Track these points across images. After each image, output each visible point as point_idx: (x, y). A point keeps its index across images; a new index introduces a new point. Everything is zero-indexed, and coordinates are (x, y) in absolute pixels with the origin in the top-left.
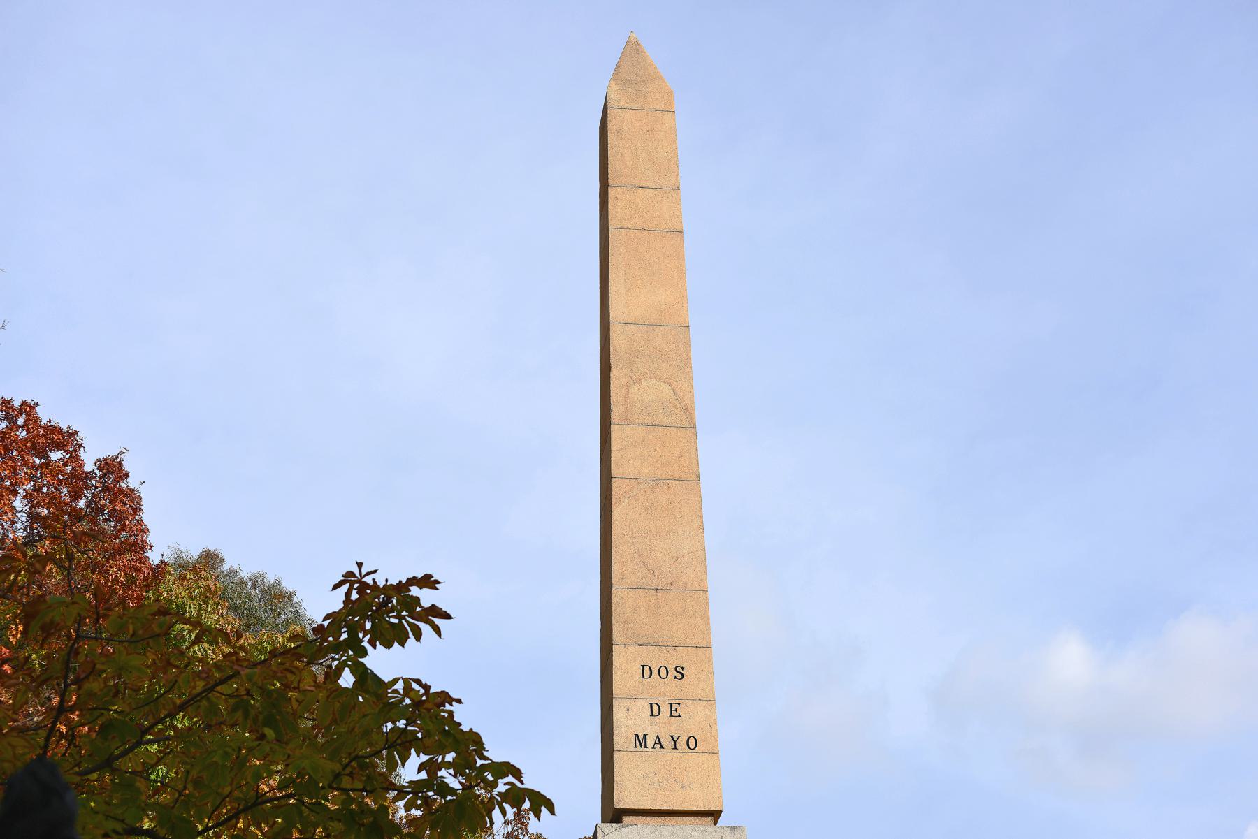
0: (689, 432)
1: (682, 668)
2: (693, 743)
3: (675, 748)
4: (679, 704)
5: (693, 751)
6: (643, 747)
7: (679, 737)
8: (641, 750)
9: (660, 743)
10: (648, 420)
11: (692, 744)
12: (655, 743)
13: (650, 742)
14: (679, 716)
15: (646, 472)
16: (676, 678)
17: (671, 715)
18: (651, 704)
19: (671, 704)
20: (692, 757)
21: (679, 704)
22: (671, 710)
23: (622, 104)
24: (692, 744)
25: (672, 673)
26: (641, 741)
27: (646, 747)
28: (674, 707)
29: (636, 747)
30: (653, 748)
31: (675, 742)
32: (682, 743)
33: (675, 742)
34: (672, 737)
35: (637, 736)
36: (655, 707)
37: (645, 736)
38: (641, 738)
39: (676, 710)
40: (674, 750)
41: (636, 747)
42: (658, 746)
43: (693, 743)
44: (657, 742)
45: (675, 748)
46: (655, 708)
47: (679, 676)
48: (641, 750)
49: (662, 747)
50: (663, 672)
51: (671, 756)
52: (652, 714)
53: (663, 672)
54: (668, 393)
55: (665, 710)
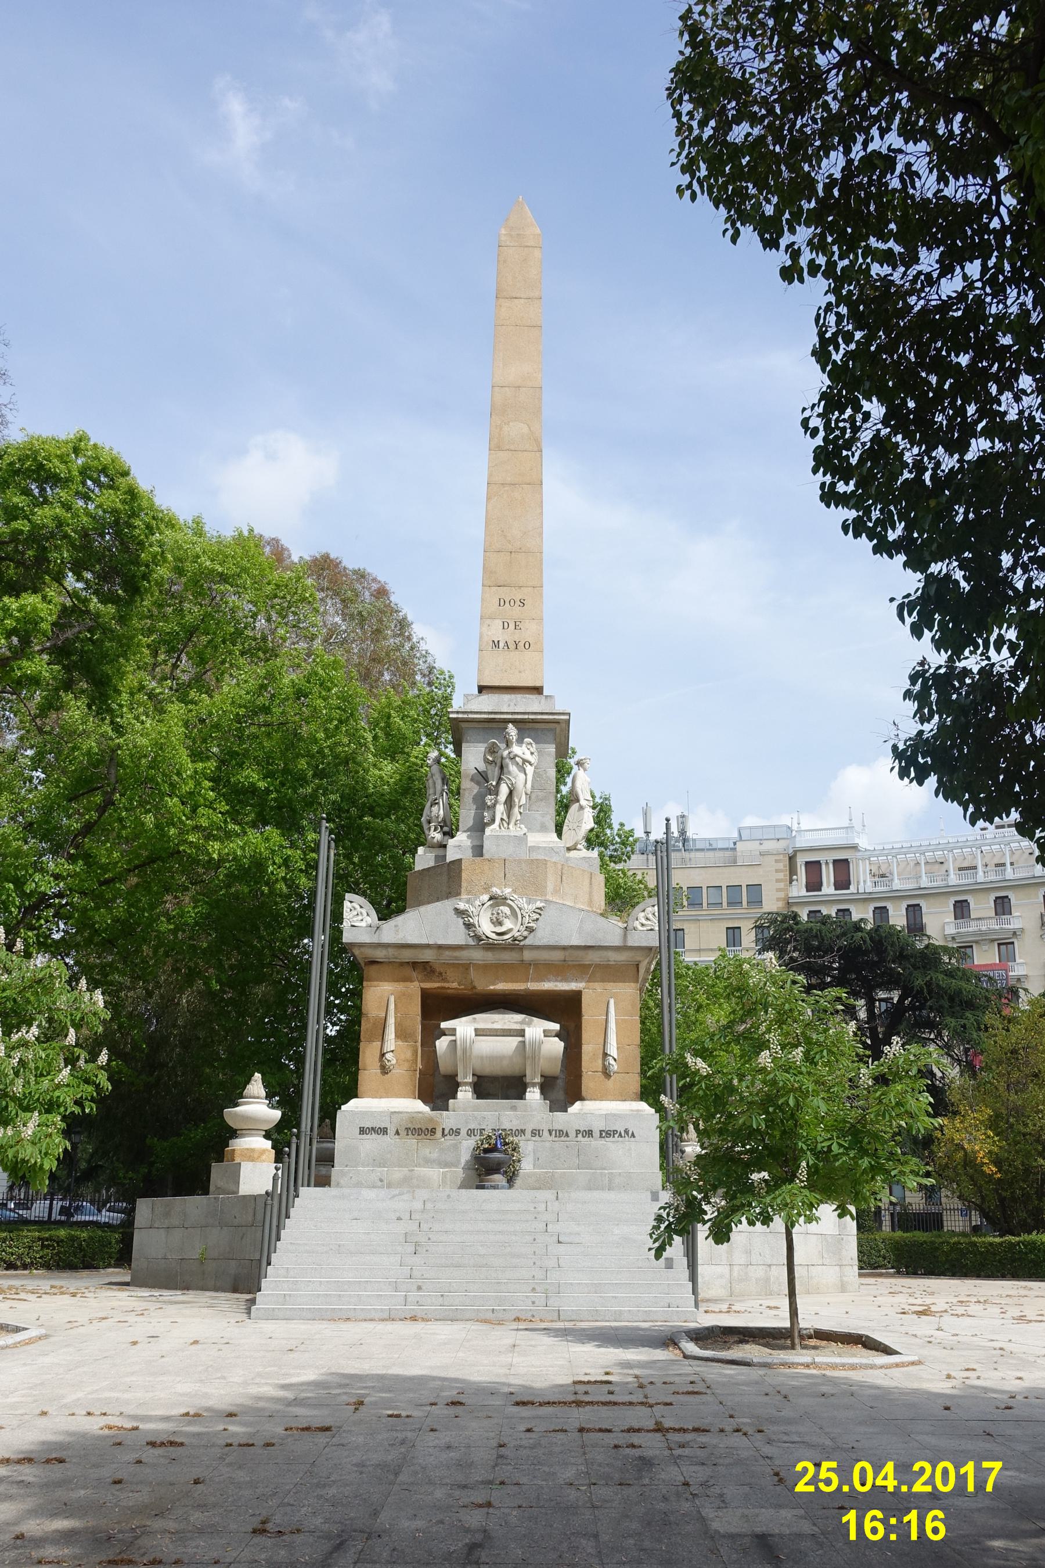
0: (538, 454)
2: (527, 646)
10: (512, 447)
11: (527, 646)
13: (501, 645)
15: (509, 480)
20: (526, 652)
23: (508, 243)
24: (527, 646)
32: (521, 644)
43: (527, 646)
50: (512, 602)
51: (514, 655)
53: (512, 602)
54: (525, 429)
55: (512, 626)
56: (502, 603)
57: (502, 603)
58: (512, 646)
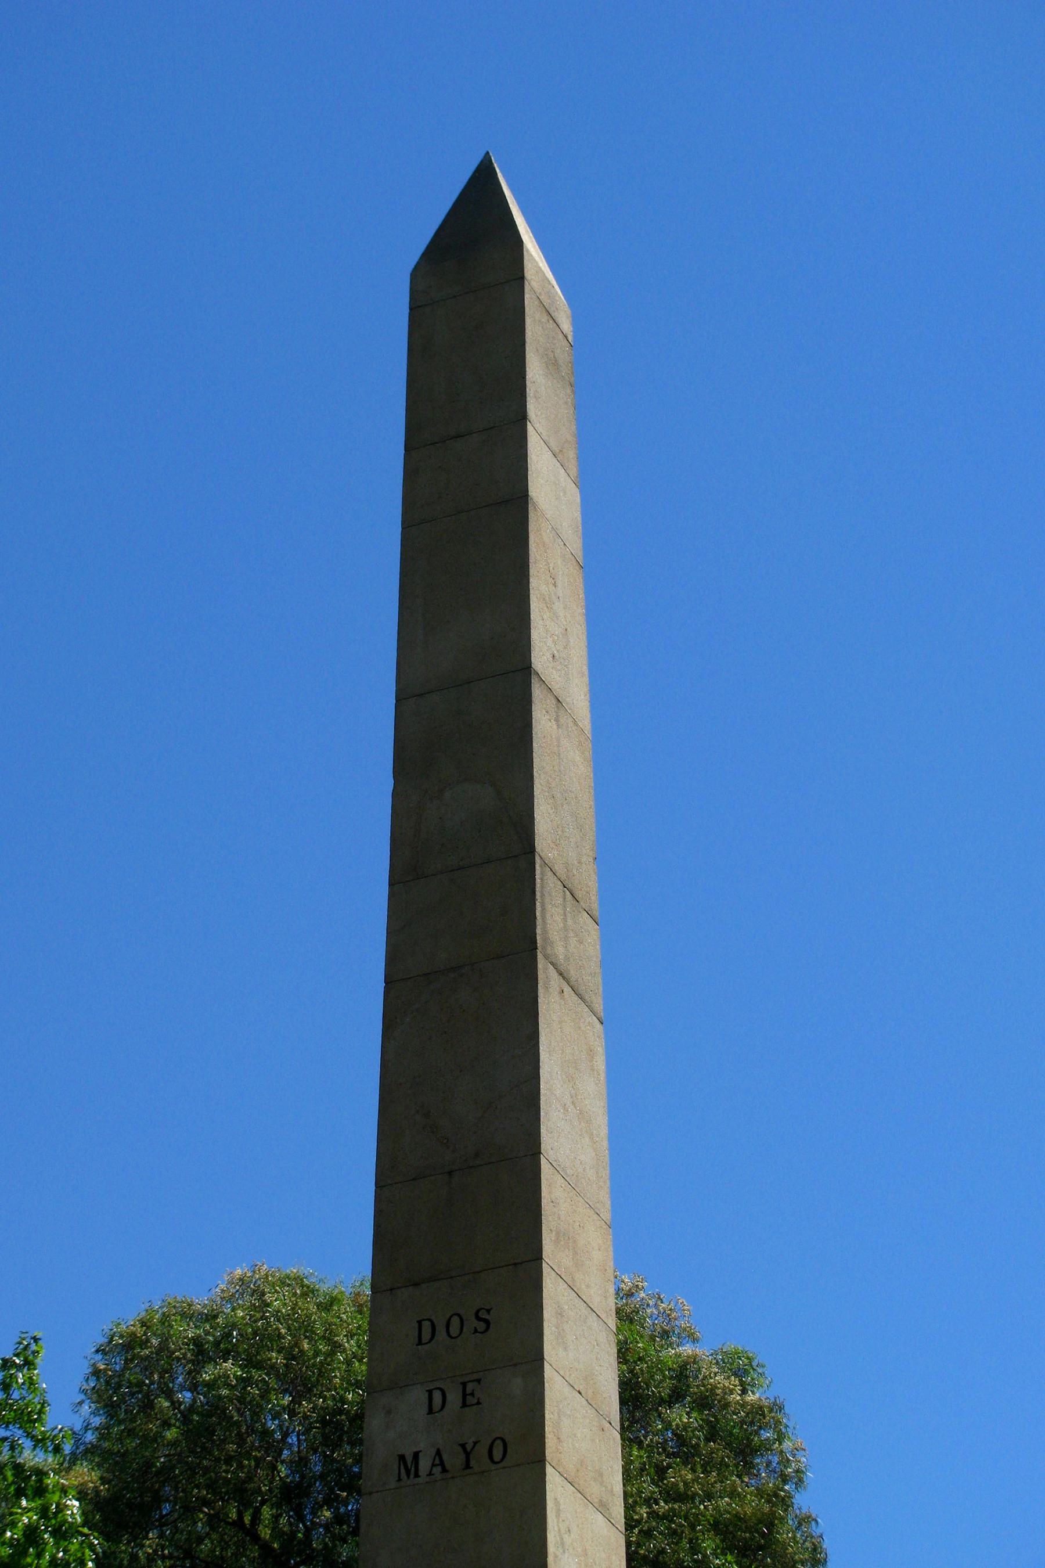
1: (488, 1311)
3: (468, 1466)
4: (479, 1381)
5: (503, 1464)
6: (412, 1476)
7: (475, 1443)
8: (409, 1482)
9: (442, 1463)
11: (497, 1454)
12: (433, 1465)
13: (424, 1464)
14: (478, 1403)
16: (476, 1331)
17: (464, 1405)
18: (430, 1392)
19: (464, 1385)
21: (479, 1381)
22: (464, 1395)
25: (472, 1323)
26: (408, 1465)
27: (417, 1475)
28: (470, 1387)
29: (399, 1480)
30: (430, 1474)
31: (468, 1455)
32: (482, 1450)
33: (468, 1455)
34: (463, 1446)
35: (402, 1458)
36: (437, 1397)
37: (416, 1456)
38: (409, 1461)
39: (472, 1394)
40: (468, 1471)
41: (399, 1480)
42: (437, 1470)
44: (437, 1461)
45: (468, 1466)
46: (437, 1397)
47: (481, 1325)
48: (409, 1482)
49: (444, 1470)
52: (430, 1411)
55: (454, 1398)
56: (426, 1335)
57: (426, 1335)
58: (454, 1460)
